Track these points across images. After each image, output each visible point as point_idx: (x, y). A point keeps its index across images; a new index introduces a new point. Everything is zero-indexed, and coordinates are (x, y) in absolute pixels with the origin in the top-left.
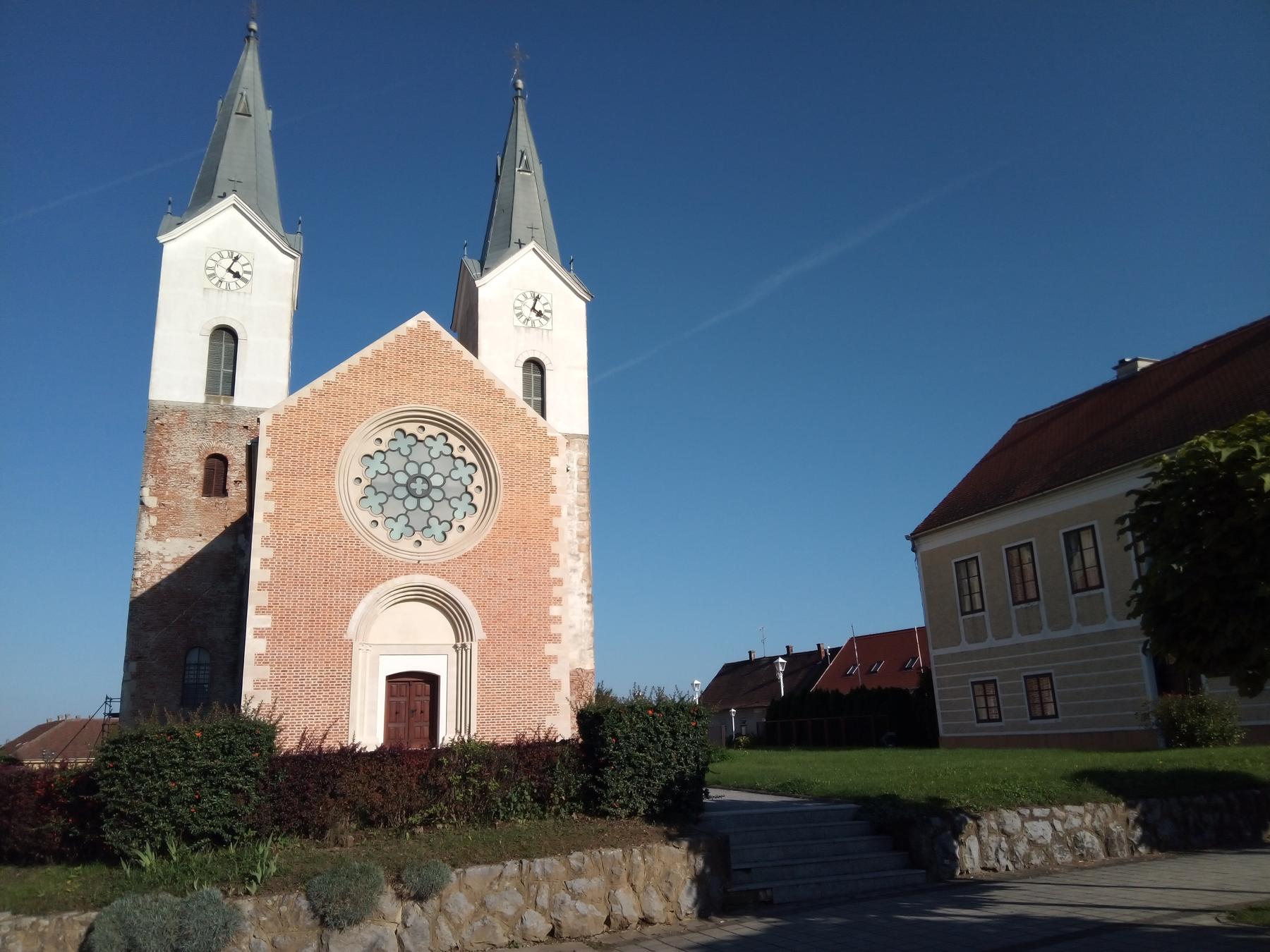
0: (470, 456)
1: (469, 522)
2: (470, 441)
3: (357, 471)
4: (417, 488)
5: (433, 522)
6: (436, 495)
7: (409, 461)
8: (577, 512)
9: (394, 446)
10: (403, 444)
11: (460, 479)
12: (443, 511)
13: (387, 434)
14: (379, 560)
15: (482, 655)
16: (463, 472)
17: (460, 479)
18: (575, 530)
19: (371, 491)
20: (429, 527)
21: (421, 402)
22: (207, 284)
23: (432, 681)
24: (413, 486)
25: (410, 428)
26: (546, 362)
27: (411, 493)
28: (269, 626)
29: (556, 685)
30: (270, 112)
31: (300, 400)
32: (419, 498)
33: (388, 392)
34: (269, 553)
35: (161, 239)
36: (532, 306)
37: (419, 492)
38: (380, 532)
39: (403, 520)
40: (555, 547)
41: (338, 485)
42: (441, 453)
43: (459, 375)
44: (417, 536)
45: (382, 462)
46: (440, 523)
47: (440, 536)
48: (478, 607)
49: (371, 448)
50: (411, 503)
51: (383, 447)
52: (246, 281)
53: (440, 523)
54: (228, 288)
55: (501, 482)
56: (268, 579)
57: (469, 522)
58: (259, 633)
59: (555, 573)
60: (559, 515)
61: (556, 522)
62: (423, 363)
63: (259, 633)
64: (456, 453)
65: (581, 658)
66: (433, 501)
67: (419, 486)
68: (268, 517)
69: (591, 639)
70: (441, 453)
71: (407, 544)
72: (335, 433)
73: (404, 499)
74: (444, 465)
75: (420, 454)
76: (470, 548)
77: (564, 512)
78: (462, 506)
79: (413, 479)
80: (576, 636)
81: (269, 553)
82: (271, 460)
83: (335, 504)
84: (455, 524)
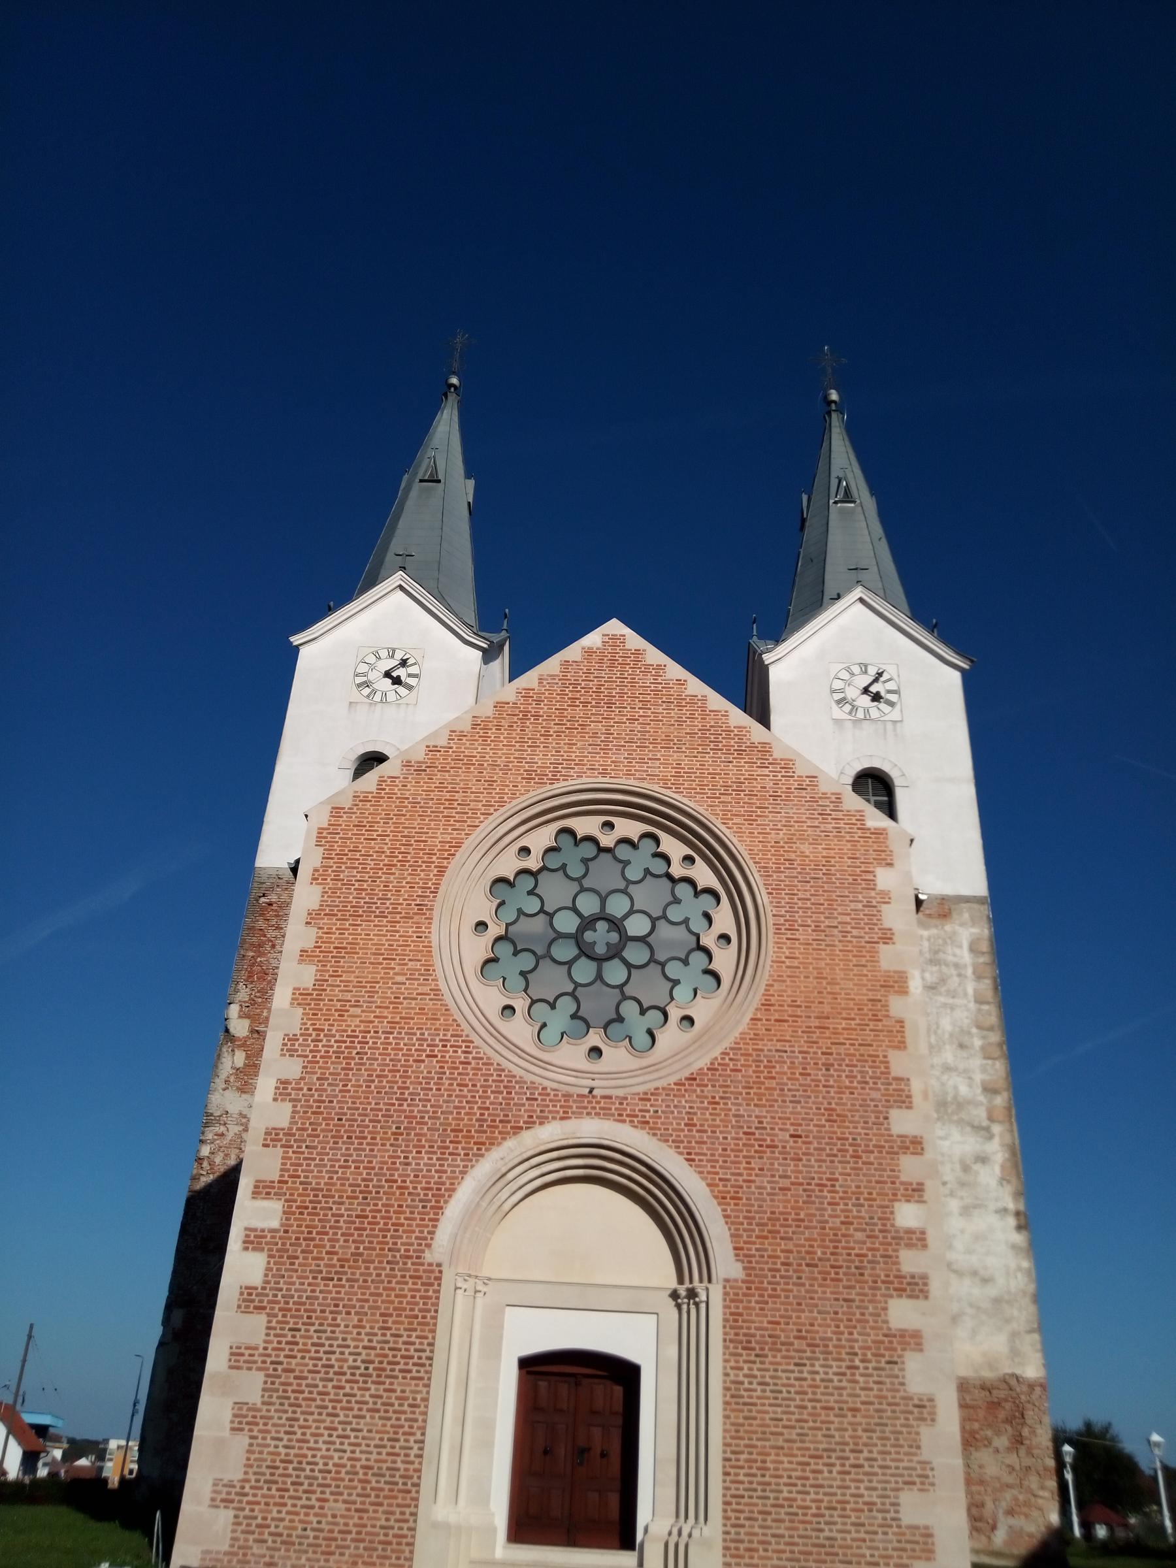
0: (704, 875)
1: (702, 1010)
2: (704, 844)
3: (483, 907)
4: (599, 943)
5: (629, 1009)
6: (636, 954)
7: (583, 890)
8: (978, 1043)
9: (554, 862)
10: (572, 857)
11: (686, 921)
12: (648, 987)
13: (541, 839)
14: (507, 1084)
15: (733, 1319)
16: (691, 907)
17: (686, 921)
18: (978, 1077)
19: (505, 950)
21: (604, 774)
22: (356, 695)
23: (625, 1375)
24: (589, 936)
25: (586, 826)
26: (894, 774)
27: (585, 951)
28: (275, 1224)
29: (924, 1408)
30: (471, 483)
31: (381, 781)
32: (600, 960)
33: (541, 759)
34: (293, 1068)
35: (296, 640)
36: (867, 689)
37: (601, 950)
38: (520, 1030)
40: (899, 1064)
41: (440, 933)
42: (647, 872)
43: (680, 722)
44: (595, 1038)
45: (531, 893)
46: (643, 1012)
47: (642, 1039)
48: (721, 1199)
49: (508, 865)
50: (584, 971)
51: (533, 863)
52: (410, 688)
53: (643, 1012)
54: (384, 700)
55: (768, 922)
56: (285, 1124)
57: (702, 1010)
58: (254, 1241)
59: (902, 1123)
60: (903, 991)
61: (897, 1006)
62: (610, 704)
63: (254, 1241)
64: (677, 870)
65: (1015, 1353)
66: (629, 966)
67: (601, 936)
68: (301, 997)
69: (1032, 1309)
70: (647, 872)
71: (572, 1055)
72: (439, 836)
73: (570, 964)
74: (650, 896)
75: (604, 875)
76: (703, 1062)
77: (915, 985)
78: (689, 976)
79: (588, 923)
80: (997, 1301)
81: (293, 1068)
82: (317, 890)
83: (428, 969)
84: (675, 1013)
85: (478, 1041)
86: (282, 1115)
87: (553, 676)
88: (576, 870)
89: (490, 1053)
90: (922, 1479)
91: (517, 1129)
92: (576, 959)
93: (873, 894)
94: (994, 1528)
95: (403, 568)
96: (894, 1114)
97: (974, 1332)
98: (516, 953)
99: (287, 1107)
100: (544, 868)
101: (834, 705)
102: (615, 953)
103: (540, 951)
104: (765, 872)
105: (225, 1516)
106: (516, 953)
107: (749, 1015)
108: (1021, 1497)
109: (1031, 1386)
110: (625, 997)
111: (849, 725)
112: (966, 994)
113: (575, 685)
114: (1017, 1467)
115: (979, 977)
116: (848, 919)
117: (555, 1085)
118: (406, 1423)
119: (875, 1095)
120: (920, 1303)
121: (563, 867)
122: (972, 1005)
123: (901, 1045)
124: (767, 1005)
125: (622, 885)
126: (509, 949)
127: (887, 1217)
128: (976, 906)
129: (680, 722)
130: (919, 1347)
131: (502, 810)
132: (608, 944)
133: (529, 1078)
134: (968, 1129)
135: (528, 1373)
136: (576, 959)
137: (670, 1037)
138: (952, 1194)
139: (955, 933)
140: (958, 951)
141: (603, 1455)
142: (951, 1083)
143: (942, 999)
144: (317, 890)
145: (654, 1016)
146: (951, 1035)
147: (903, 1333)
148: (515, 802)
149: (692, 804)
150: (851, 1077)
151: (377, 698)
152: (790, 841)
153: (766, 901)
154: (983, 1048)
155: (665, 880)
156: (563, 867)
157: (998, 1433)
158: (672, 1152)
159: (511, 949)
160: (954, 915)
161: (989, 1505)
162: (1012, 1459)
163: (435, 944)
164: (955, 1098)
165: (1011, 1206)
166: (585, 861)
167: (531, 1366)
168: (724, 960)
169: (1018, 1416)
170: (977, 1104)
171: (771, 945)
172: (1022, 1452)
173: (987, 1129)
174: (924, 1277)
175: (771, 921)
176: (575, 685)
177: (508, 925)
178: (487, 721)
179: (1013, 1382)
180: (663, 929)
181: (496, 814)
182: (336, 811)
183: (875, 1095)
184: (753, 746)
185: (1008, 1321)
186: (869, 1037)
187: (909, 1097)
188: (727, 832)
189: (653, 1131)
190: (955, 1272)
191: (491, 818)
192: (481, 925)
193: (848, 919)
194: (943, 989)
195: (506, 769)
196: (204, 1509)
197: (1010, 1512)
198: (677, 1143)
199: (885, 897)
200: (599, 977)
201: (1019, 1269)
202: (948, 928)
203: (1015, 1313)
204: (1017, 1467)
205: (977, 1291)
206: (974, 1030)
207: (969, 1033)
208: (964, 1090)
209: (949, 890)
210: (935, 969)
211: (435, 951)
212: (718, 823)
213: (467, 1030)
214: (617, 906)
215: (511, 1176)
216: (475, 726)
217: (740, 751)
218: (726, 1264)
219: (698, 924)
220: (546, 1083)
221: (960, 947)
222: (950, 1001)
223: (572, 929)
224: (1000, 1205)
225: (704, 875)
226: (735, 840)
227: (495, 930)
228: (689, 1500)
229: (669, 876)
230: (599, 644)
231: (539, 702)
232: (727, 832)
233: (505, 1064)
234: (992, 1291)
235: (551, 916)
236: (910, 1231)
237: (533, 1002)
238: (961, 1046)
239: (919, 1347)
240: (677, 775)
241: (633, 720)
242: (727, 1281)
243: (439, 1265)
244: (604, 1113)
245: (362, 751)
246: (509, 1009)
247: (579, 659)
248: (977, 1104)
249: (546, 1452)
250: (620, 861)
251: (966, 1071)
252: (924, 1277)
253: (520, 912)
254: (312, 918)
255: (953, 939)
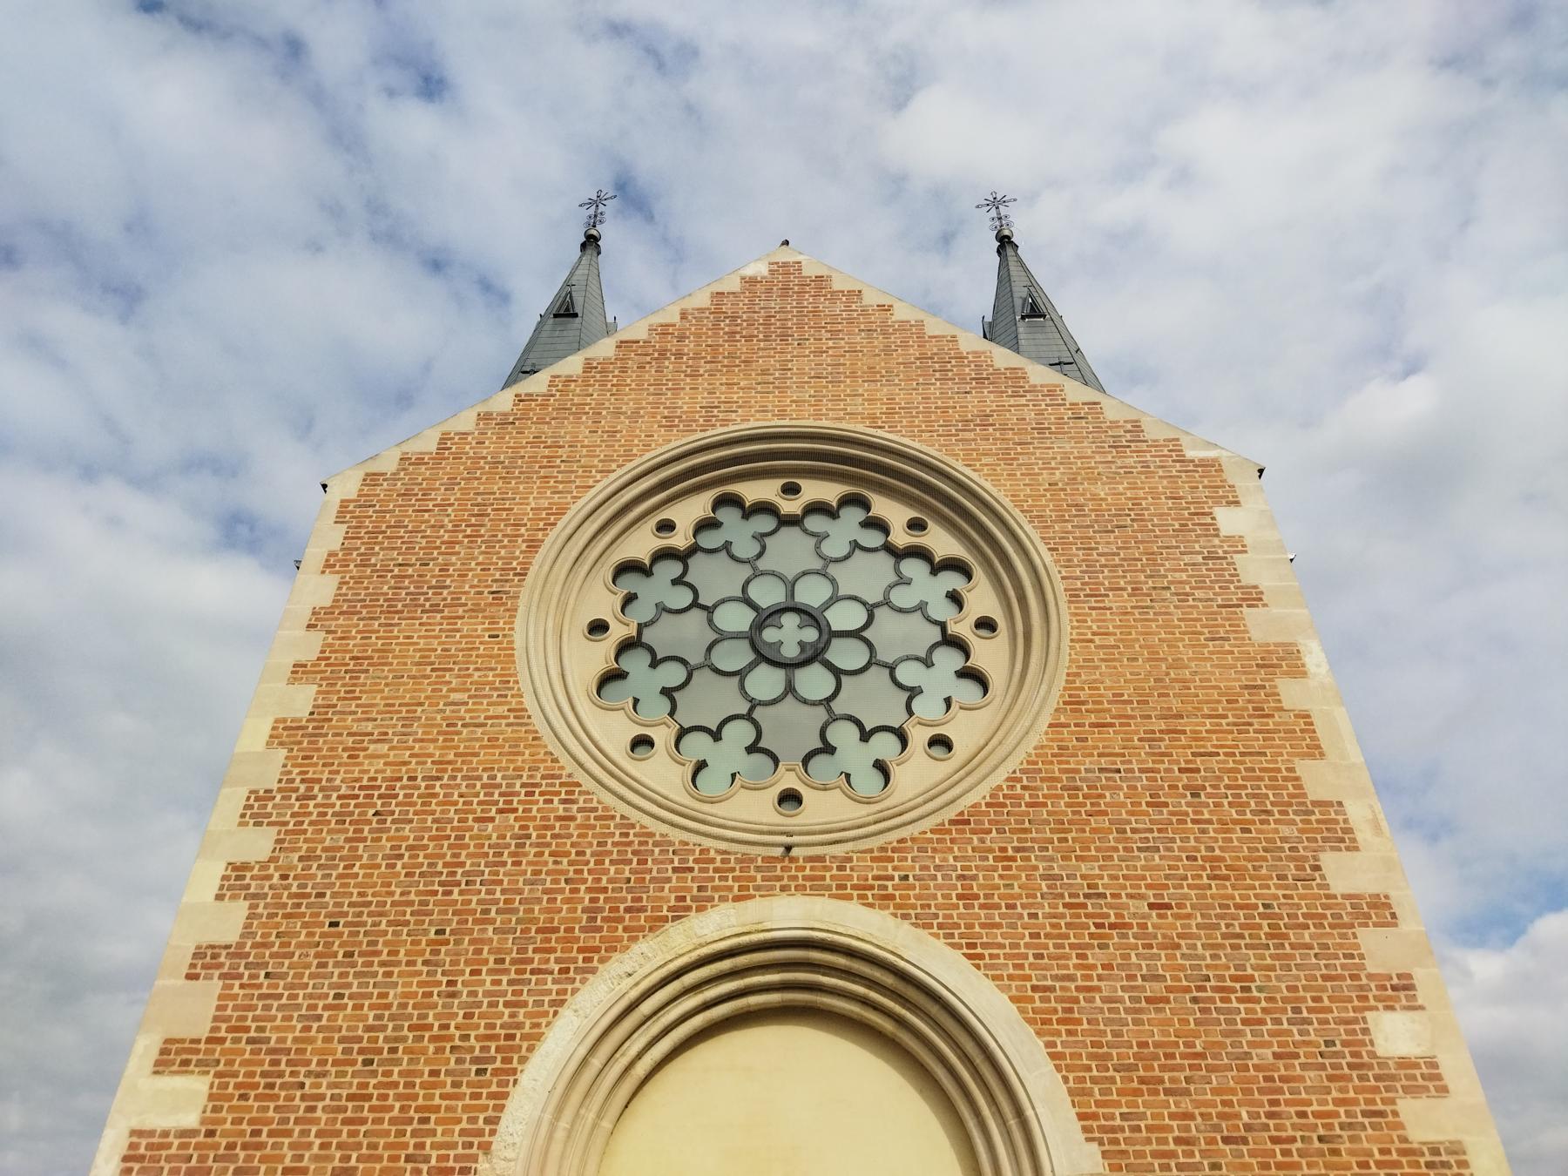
0: (941, 542)
5: (842, 735)
6: (847, 655)
12: (871, 699)
16: (928, 588)
20: (828, 749)
21: (782, 415)
24: (770, 635)
27: (764, 656)
28: (191, 1120)
32: (790, 666)
38: (662, 773)
39: (740, 733)
40: (1317, 780)
41: (529, 630)
42: (856, 545)
43: (887, 351)
46: (865, 736)
48: (1041, 1023)
49: (642, 544)
50: (765, 682)
51: (680, 540)
53: (865, 736)
55: (1058, 588)
56: (232, 937)
57: (965, 731)
59: (1345, 874)
60: (1298, 671)
61: (1291, 693)
62: (784, 337)
64: (901, 538)
66: (837, 673)
67: (789, 635)
72: (534, 500)
76: (979, 795)
77: (1315, 657)
84: (919, 737)
89: (609, 799)
91: (656, 923)
92: (752, 666)
93: (1216, 541)
99: (240, 909)
102: (814, 655)
104: (1038, 519)
110: (834, 718)
113: (734, 318)
116: (1184, 576)
117: (723, 846)
119: (1285, 831)
123: (1315, 751)
124: (1073, 703)
125: (817, 564)
127: (1359, 1040)
129: (887, 351)
131: (630, 465)
132: (801, 643)
133: (676, 836)
137: (916, 772)
145: (884, 746)
156: (727, 546)
159: (648, 659)
163: (518, 643)
166: (761, 537)
168: (989, 654)
175: (1060, 586)
176: (734, 318)
177: (641, 627)
181: (620, 472)
183: (1285, 831)
187: (1349, 831)
188: (974, 476)
191: (613, 476)
193: (1184, 576)
198: (947, 930)
200: (790, 689)
211: (519, 654)
212: (959, 465)
214: (812, 593)
215: (647, 1007)
225: (941, 542)
226: (988, 485)
229: (889, 548)
231: (681, 338)
233: (635, 816)
235: (710, 610)
236: (1405, 1063)
237: (683, 733)
240: (890, 413)
244: (815, 886)
246: (642, 743)
250: (813, 534)
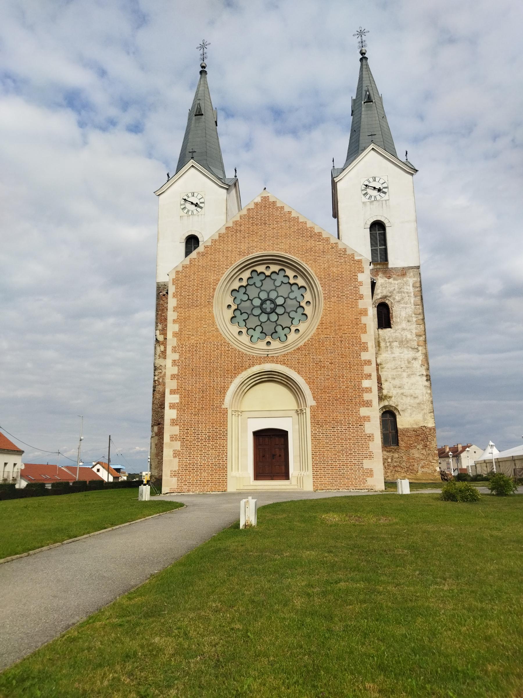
0: (301, 282)
1: (302, 327)
2: (300, 272)
3: (229, 300)
4: (269, 308)
5: (279, 329)
6: (280, 310)
7: (261, 291)
8: (414, 319)
10: (257, 280)
11: (296, 298)
12: (284, 321)
13: (246, 275)
14: (242, 355)
15: (313, 417)
16: (297, 293)
17: (296, 298)
18: (414, 331)
19: (238, 313)
20: (276, 332)
21: (265, 250)
22: (182, 213)
23: (283, 435)
24: (264, 306)
25: (260, 269)
27: (263, 311)
28: (178, 401)
29: (370, 437)
31: (191, 260)
32: (268, 314)
33: (243, 247)
34: (176, 356)
37: (268, 310)
38: (245, 339)
39: (259, 329)
41: (216, 311)
42: (282, 282)
43: (290, 227)
44: (268, 339)
45: (244, 293)
46: (283, 329)
47: (283, 338)
48: (309, 383)
49: (236, 285)
51: (244, 283)
52: (201, 208)
53: (283, 329)
54: (193, 214)
55: (322, 296)
56: (176, 373)
57: (302, 327)
58: (172, 406)
60: (366, 315)
62: (265, 224)
63: (172, 406)
64: (292, 281)
65: (425, 419)
66: (278, 315)
67: (268, 306)
68: (175, 334)
70: (282, 282)
71: (262, 345)
72: (212, 278)
73: (259, 316)
74: (284, 290)
75: (268, 284)
76: (302, 344)
78: (297, 316)
79: (263, 302)
80: (419, 404)
81: (176, 356)
82: (175, 300)
83: (214, 323)
84: (293, 329)
85: (231, 344)
86: (175, 370)
87: (245, 215)
88: (258, 284)
89: (236, 346)
90: (370, 456)
91: (246, 369)
92: (261, 314)
93: (357, 283)
94: (417, 472)
95: (192, 158)
96: (362, 354)
97: (411, 414)
98: (241, 314)
99: (176, 368)
100: (248, 285)
101: (362, 196)
102: (273, 311)
103: (249, 312)
104: (320, 279)
105: (175, 479)
106: (241, 314)
107: (316, 327)
108: (426, 463)
109: (430, 429)
110: (277, 325)
111: (368, 203)
112: (411, 303)
113: (253, 218)
114: (425, 454)
115: (415, 296)
116: (348, 292)
117: (256, 355)
118: (222, 452)
119: (356, 348)
120: (370, 408)
121: (254, 284)
122: (413, 307)
123: (365, 332)
124: (322, 323)
125: (274, 288)
126: (239, 312)
128: (415, 270)
129: (290, 227)
130: (369, 421)
131: (232, 266)
132: (271, 308)
133: (248, 353)
134: (410, 349)
135: (256, 436)
136: (261, 314)
137: (292, 337)
138: (404, 371)
139: (407, 281)
140: (408, 287)
141: (280, 456)
142: (405, 334)
143: (402, 305)
144: (175, 300)
145: (287, 330)
146: (405, 318)
147: (364, 417)
148: (236, 263)
149: (295, 258)
150: (349, 344)
151: (190, 213)
152: (329, 268)
153: (321, 289)
154: (416, 321)
155: (288, 284)
156: (254, 284)
157: (418, 444)
158: (293, 371)
159: (240, 313)
160: (407, 274)
161: (416, 465)
162: (424, 452)
163: (215, 314)
164: (406, 339)
165: (425, 373)
166: (262, 281)
167: (257, 434)
168: (308, 310)
169: (425, 439)
170: (413, 341)
171: (323, 304)
172: (427, 449)
173: (417, 349)
174: (371, 401)
175: (323, 296)
176: (253, 218)
177: (238, 305)
178: (224, 234)
179: (424, 428)
180: (289, 301)
181: (230, 268)
182: (177, 272)
183: (356, 348)
184: (315, 234)
185: (422, 410)
186: (355, 331)
187: (367, 348)
188: (307, 266)
189: (287, 366)
190: (405, 396)
191: (228, 270)
192: (229, 306)
193: (348, 292)
194: (402, 302)
195: (232, 252)
196: (169, 478)
197: (423, 467)
198: (295, 369)
199: (361, 284)
200: (268, 319)
201: (427, 393)
202: (405, 279)
203: (425, 407)
204: (425, 454)
205: (412, 401)
206: (413, 315)
207: (411, 316)
208: (409, 336)
209: (406, 265)
210: (400, 295)
211: (215, 316)
212: (304, 263)
213: (228, 340)
214: (273, 295)
215: (245, 382)
216: (220, 237)
217: (311, 236)
218: (311, 401)
219: (299, 298)
220: (254, 354)
221: (409, 286)
222: (405, 306)
223: (259, 304)
224: (421, 373)
225: (301, 282)
226: (310, 269)
227: (234, 307)
228: (302, 467)
229: (289, 283)
230: (260, 201)
231: (241, 226)
232: (307, 266)
233: (240, 350)
234: (417, 401)
235: (252, 300)
236: (367, 388)
237: (248, 329)
238: (408, 321)
239: (369, 421)
240: (290, 248)
241: (273, 229)
242: (311, 406)
243: (227, 409)
244: (273, 362)
245: (187, 235)
246: (240, 332)
247: (253, 207)
248: (413, 341)
249: (263, 456)
250: (273, 280)
251: (410, 330)
252: (371, 401)
253: (242, 300)
254: (175, 309)
255: (406, 283)
